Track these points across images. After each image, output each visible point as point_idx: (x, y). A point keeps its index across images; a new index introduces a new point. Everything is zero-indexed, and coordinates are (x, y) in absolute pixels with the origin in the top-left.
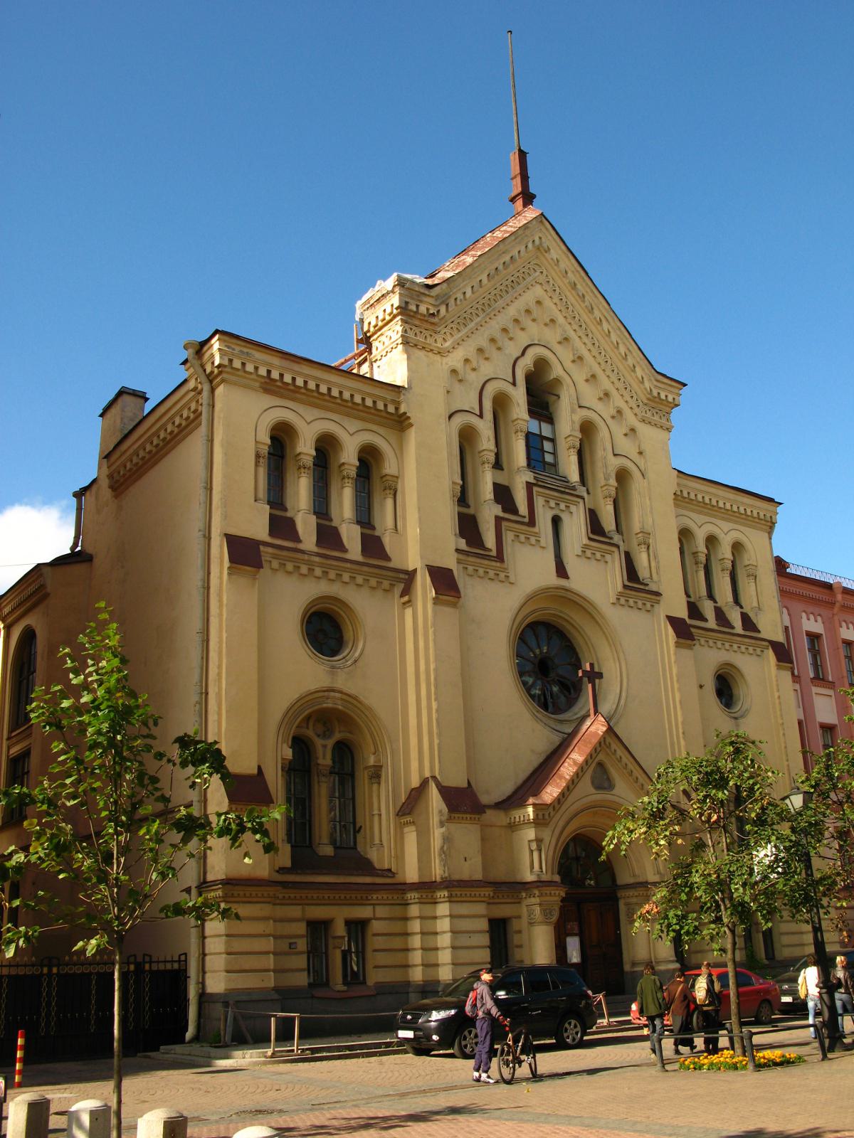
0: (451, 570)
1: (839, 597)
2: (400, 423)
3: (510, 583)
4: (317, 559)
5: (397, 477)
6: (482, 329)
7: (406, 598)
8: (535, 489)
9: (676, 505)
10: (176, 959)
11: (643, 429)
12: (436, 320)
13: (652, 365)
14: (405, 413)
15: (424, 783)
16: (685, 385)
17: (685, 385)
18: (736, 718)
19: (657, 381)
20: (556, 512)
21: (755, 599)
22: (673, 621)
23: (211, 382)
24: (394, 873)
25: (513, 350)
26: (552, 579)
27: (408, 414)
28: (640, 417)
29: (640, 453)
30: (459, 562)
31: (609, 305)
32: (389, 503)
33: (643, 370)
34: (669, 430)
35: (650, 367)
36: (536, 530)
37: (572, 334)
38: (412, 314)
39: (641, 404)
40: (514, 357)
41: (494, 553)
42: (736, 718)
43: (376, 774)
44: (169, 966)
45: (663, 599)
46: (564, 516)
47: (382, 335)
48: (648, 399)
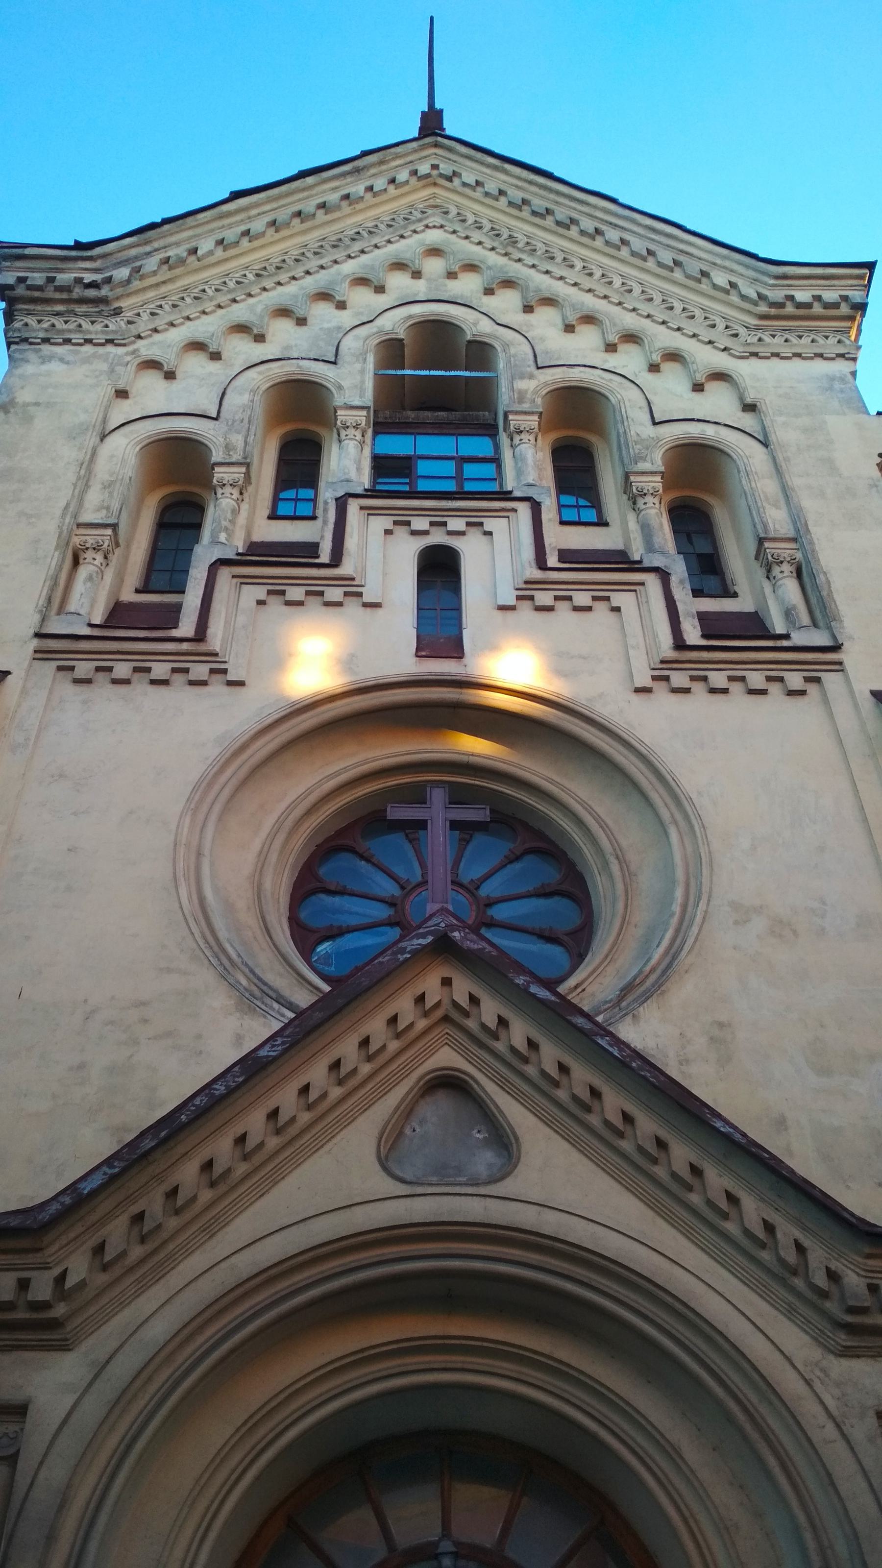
3: (230, 683)
6: (251, 301)
11: (744, 369)
12: (105, 291)
16: (871, 266)
19: (777, 277)
20: (437, 538)
29: (750, 408)
30: (41, 655)
31: (614, 201)
35: (753, 262)
36: (346, 568)
37: (515, 270)
38: (37, 294)
39: (742, 331)
45: (846, 656)
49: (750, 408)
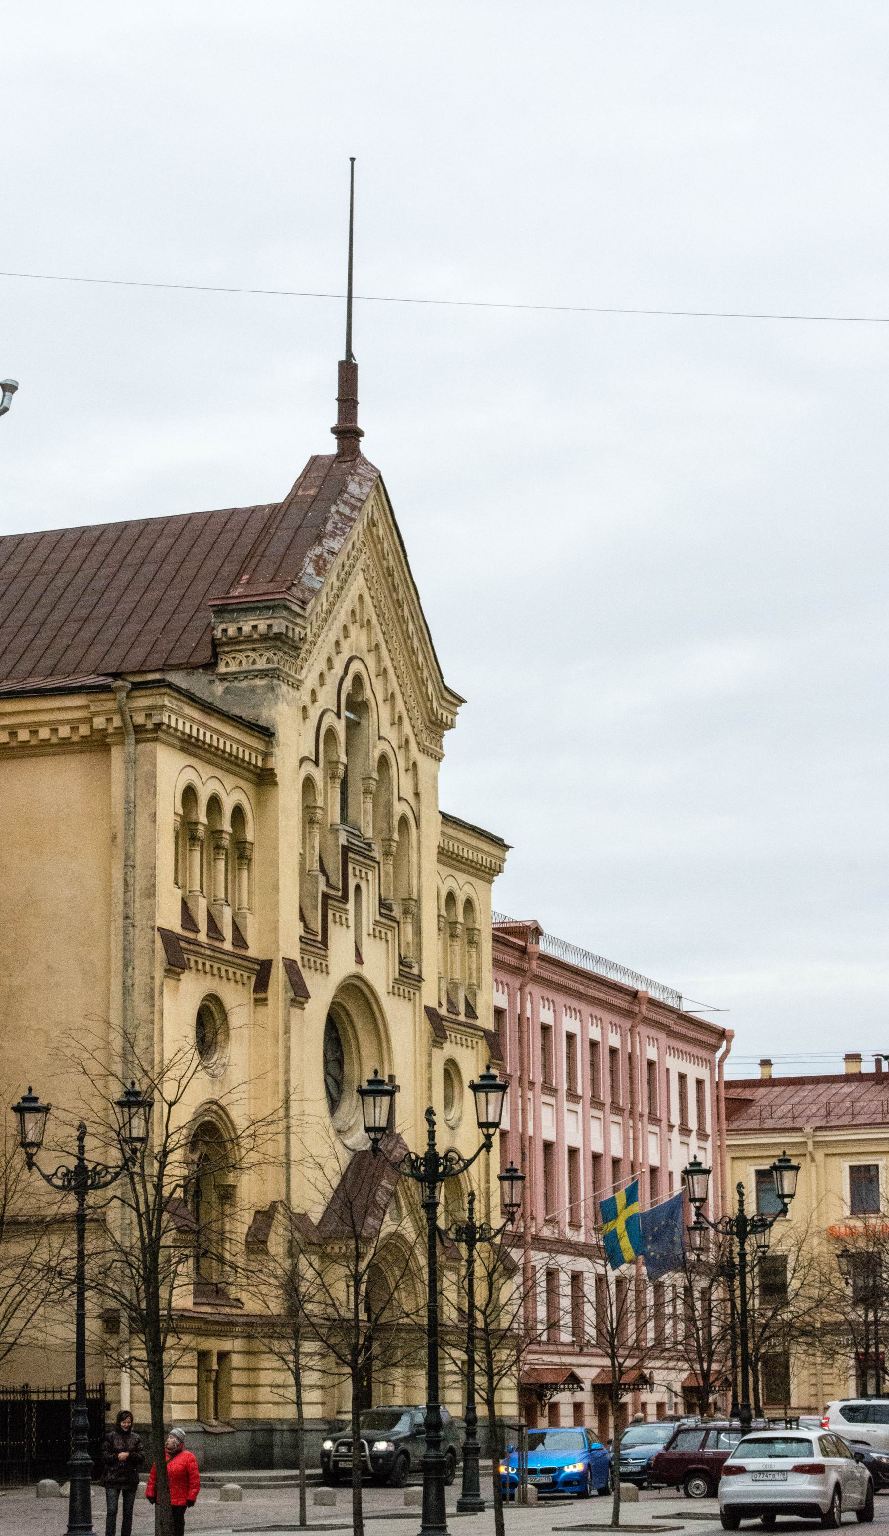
0: (295, 962)
1: (534, 963)
2: (264, 779)
4: (208, 952)
5: (252, 844)
7: (262, 996)
8: (350, 855)
9: (439, 861)
10: (66, 1388)
13: (442, 677)
14: (272, 769)
15: (273, 1206)
17: (465, 701)
18: (453, 1129)
21: (474, 974)
22: (430, 1013)
23: (136, 732)
24: (242, 1304)
25: (339, 669)
26: (351, 968)
27: (276, 771)
28: (422, 747)
32: (245, 873)
33: (434, 688)
34: (439, 760)
40: (339, 677)
41: (319, 938)
42: (453, 1129)
43: (227, 1195)
44: (57, 1397)
46: (363, 885)
47: (240, 651)
48: (430, 721)
49: (417, 795)
